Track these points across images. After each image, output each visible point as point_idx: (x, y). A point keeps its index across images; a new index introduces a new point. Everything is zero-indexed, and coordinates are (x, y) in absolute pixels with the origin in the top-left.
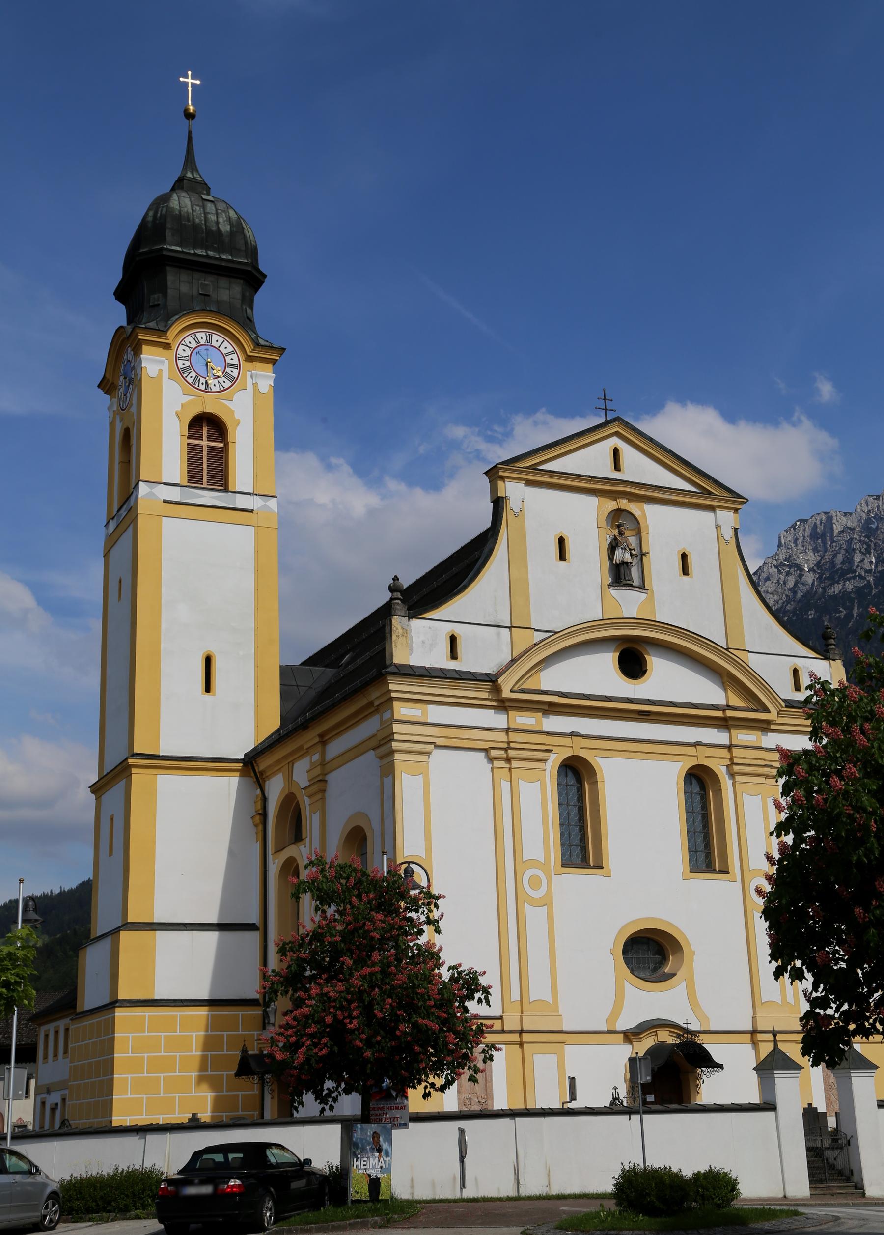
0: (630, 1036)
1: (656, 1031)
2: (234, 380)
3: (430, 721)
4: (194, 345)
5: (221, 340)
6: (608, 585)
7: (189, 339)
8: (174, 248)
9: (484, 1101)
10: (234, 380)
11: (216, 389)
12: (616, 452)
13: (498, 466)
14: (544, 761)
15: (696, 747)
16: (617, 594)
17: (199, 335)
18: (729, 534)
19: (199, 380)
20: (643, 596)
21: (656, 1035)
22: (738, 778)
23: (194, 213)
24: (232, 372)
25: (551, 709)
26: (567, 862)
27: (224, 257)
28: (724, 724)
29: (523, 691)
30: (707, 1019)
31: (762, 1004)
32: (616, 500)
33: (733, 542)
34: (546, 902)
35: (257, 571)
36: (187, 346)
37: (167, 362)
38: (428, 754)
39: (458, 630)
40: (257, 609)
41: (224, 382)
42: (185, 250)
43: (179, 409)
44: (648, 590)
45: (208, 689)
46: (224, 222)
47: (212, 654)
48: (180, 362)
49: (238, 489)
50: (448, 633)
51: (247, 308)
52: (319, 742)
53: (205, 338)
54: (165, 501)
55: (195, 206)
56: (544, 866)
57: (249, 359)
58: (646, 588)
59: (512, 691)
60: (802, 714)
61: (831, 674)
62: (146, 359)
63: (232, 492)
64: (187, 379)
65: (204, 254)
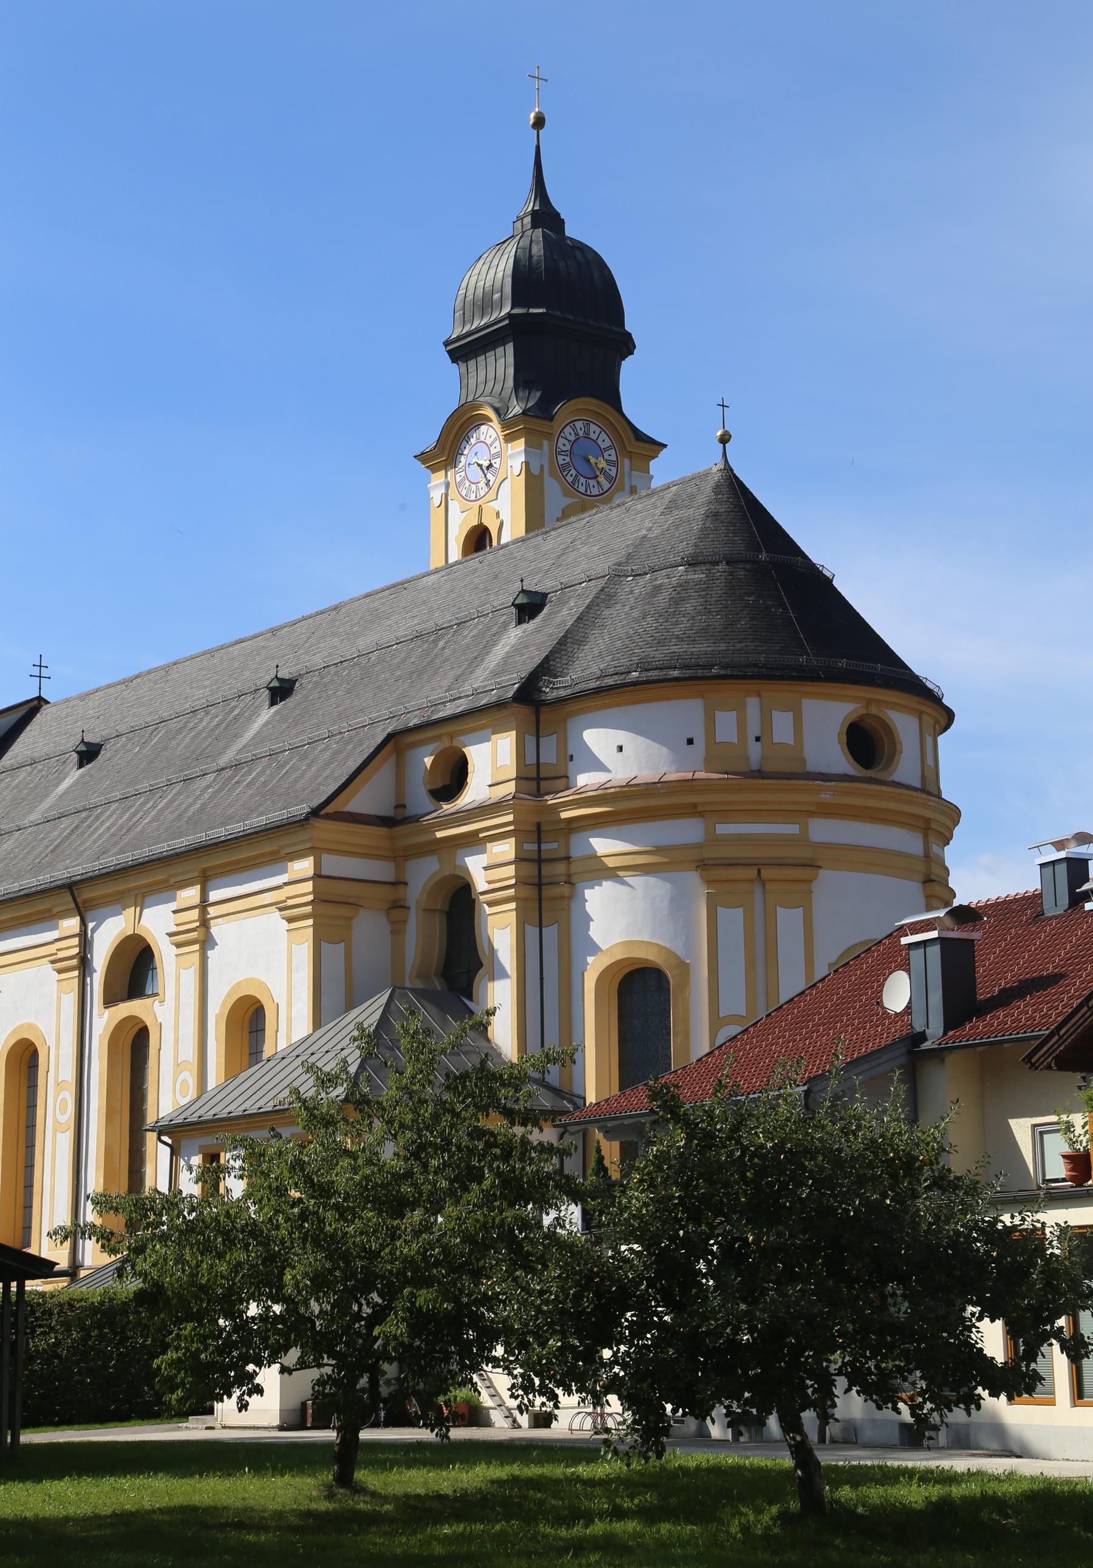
4: (572, 438)
48: (560, 458)
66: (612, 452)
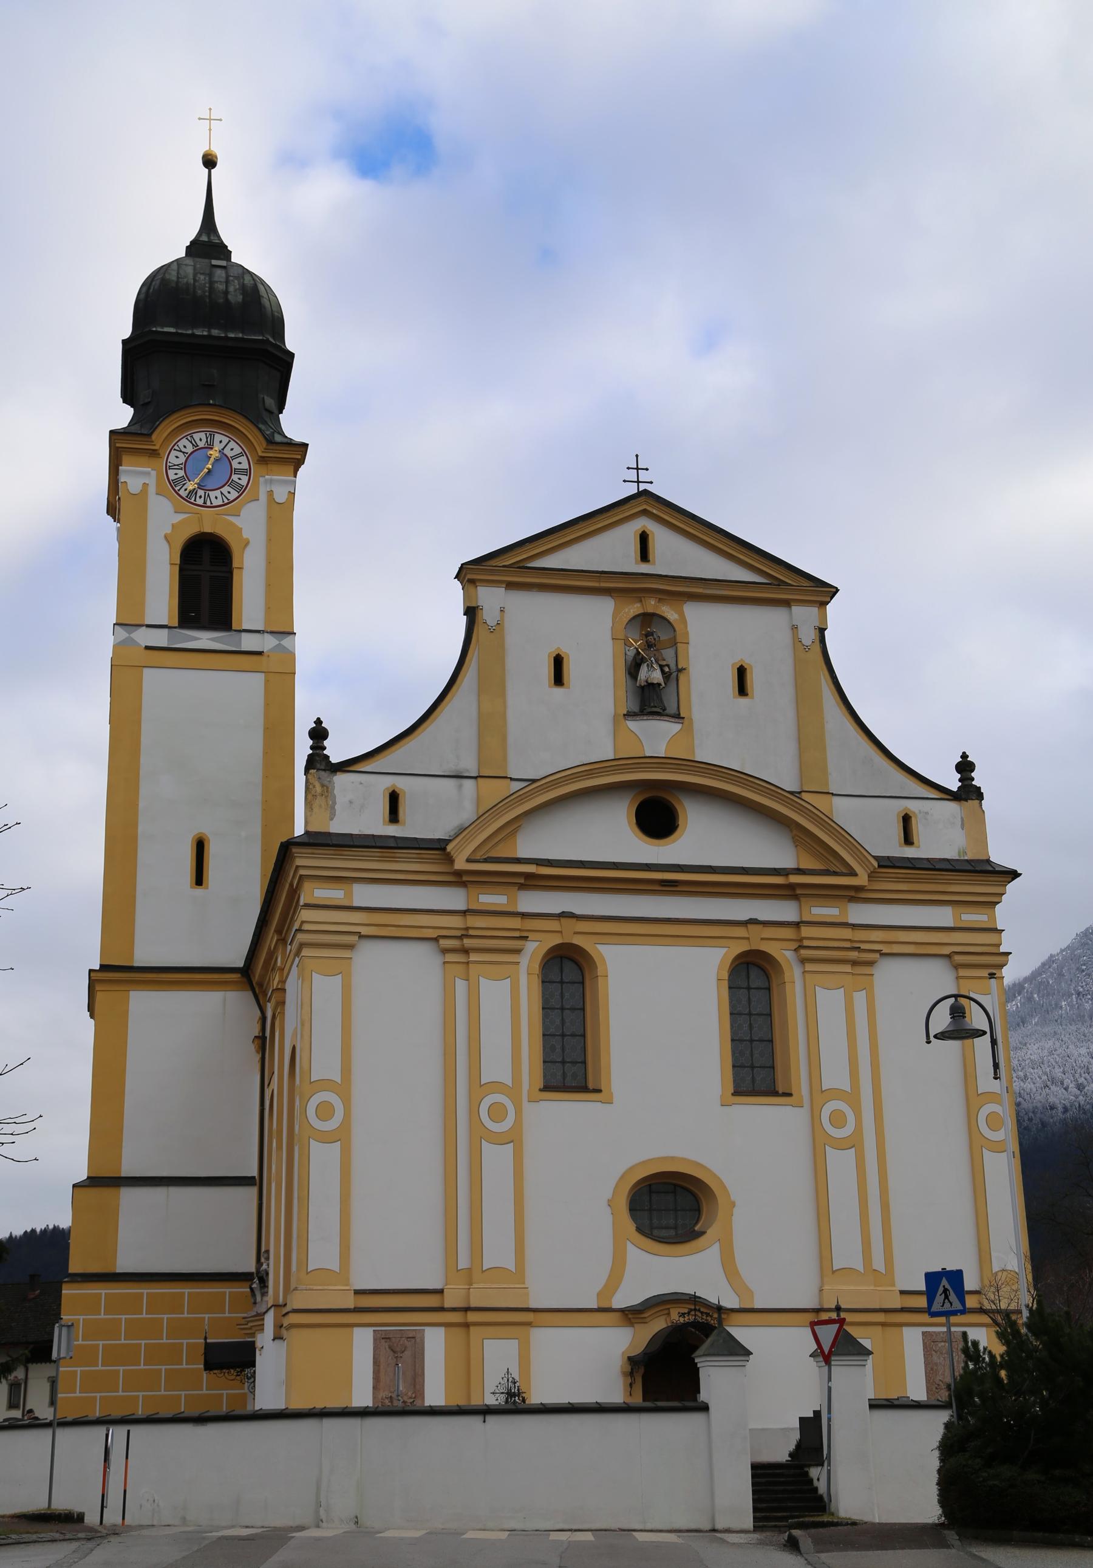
0: (632, 1315)
1: (669, 1309)
2: (241, 489)
3: (355, 904)
4: (190, 449)
5: (225, 440)
6: (624, 715)
7: (184, 442)
8: (166, 329)
9: (412, 1400)
10: (241, 489)
11: (219, 502)
12: (644, 538)
13: (464, 566)
14: (518, 951)
15: (747, 926)
16: (632, 725)
17: (197, 437)
18: (808, 636)
19: (197, 492)
20: (678, 727)
21: (669, 1314)
22: (809, 967)
23: (197, 284)
24: (240, 479)
25: (531, 882)
26: (550, 1086)
27: (231, 335)
28: (790, 892)
29: (486, 860)
30: (751, 1293)
31: (834, 1272)
32: (641, 601)
33: (817, 648)
34: (514, 1139)
35: (266, 729)
36: (181, 451)
37: (154, 473)
38: (351, 947)
39: (401, 783)
40: (266, 777)
41: (229, 492)
42: (180, 331)
43: (169, 530)
44: (684, 718)
45: (199, 879)
46: (235, 290)
47: (204, 837)
48: (171, 473)
49: (244, 627)
50: (387, 789)
51: (265, 397)
52: (278, 940)
53: (204, 440)
54: (147, 648)
55: (199, 275)
56: (513, 1092)
57: (263, 461)
58: (682, 715)
59: (468, 861)
60: (438, 857)
61: (962, 818)
62: (125, 471)
63: (236, 631)
64: (180, 493)
65: (205, 333)
66: (243, 459)
